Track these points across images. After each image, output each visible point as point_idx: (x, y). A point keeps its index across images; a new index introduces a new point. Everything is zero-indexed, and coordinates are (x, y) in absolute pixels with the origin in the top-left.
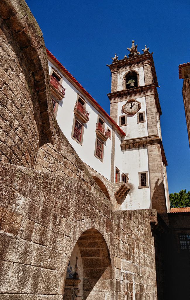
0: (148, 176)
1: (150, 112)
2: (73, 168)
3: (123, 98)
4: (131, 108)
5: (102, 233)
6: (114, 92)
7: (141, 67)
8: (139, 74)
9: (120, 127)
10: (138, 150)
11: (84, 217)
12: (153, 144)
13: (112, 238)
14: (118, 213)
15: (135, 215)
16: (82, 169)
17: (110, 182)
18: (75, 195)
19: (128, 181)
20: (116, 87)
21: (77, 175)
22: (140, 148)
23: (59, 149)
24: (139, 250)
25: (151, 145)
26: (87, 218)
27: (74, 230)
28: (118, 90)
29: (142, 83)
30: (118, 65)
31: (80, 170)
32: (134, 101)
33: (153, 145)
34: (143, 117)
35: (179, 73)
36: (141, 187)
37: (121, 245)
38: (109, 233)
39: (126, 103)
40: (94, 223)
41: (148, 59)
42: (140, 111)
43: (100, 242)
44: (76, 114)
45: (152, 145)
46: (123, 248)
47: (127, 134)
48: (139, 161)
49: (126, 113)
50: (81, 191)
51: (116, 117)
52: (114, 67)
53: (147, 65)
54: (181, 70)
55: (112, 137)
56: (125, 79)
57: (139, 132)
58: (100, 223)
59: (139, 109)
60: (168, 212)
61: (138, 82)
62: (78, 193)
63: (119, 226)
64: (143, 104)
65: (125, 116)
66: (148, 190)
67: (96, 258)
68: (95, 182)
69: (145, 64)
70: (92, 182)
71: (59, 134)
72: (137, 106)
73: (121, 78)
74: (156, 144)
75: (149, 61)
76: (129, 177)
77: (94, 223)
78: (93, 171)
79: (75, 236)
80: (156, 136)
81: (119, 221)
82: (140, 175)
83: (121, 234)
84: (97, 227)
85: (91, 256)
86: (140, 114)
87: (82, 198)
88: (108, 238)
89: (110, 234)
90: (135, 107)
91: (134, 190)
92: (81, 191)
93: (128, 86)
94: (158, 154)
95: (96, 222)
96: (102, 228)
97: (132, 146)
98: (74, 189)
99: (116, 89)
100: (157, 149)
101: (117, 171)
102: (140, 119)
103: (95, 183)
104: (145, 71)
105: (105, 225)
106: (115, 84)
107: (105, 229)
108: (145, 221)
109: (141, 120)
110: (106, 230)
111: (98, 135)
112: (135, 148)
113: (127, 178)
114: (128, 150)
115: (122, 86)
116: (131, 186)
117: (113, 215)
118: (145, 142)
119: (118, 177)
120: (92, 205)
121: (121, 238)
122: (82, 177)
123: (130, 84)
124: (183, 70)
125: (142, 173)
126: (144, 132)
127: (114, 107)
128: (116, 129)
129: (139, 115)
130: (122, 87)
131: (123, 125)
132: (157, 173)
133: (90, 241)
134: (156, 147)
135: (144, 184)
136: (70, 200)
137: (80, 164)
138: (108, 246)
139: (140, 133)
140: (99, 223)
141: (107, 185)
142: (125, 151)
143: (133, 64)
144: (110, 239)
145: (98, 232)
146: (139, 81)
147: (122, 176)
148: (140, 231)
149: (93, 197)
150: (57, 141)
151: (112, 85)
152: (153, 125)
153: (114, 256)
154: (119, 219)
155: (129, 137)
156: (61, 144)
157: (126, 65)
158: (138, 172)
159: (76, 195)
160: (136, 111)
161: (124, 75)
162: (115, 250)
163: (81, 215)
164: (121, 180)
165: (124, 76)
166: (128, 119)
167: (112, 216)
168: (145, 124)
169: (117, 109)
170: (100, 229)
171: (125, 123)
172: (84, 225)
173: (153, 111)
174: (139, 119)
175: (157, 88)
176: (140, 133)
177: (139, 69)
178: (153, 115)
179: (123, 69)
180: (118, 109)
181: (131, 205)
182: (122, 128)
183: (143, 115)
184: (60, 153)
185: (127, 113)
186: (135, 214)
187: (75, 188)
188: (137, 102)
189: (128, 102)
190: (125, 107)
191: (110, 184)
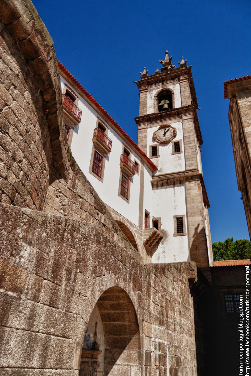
1: (188, 140)
2: (92, 211)
3: (154, 123)
4: (165, 135)
5: (127, 291)
6: (143, 115)
7: (177, 84)
8: (174, 93)
9: (150, 159)
10: (173, 188)
11: (106, 272)
13: (140, 299)
14: (148, 267)
15: (170, 270)
16: (103, 211)
17: (138, 228)
18: (94, 245)
19: (160, 228)
20: (145, 109)
21: (97, 220)
22: (176, 185)
23: (73, 187)
24: (174, 314)
25: (189, 182)
26: (109, 274)
27: (93, 288)
28: (148, 113)
29: (177, 104)
30: (148, 82)
31: (100, 213)
32: (168, 126)
33: (192, 182)
34: (179, 147)
35: (225, 91)
36: (176, 234)
37: (151, 308)
38: (137, 292)
40: (118, 280)
41: (186, 74)
42: (176, 139)
43: (126, 304)
44: (95, 143)
45: (190, 181)
46: (154, 310)
47: (159, 169)
48: (175, 201)
49: (158, 142)
50: (102, 239)
51: (146, 146)
52: (142, 83)
53: (184, 81)
54: (227, 87)
55: (141, 171)
56: (157, 99)
57: (175, 165)
58: (125, 280)
59: (175, 136)
60: (211, 265)
61: (173, 103)
62: (98, 242)
63: (149, 284)
64: (180, 131)
65: (156, 146)
66: (185, 238)
67: (120, 323)
68: (119, 228)
70: (115, 228)
71: (75, 168)
72: (171, 133)
73: (151, 97)
74: (195, 181)
75: (187, 76)
76: (162, 221)
77: (117, 279)
78: (116, 214)
79: (94, 296)
80: (196, 170)
81: (149, 278)
82: (176, 220)
83: (152, 294)
84: (122, 284)
85: (114, 321)
86: (176, 142)
87: (102, 248)
88: (135, 298)
89: (138, 293)
90: (169, 134)
91: (168, 239)
92: (102, 239)
93: (161, 108)
94: (198, 193)
95: (120, 279)
96: (128, 286)
97: (166, 183)
98: (93, 237)
99: (145, 111)
100: (197, 187)
101: (147, 215)
102: (175, 149)
103: (119, 230)
104: (182, 88)
105: (132, 282)
106: (144, 106)
107: (131, 287)
108: (181, 277)
109: (177, 150)
110: (133, 288)
111: (122, 169)
112: (169, 186)
113: (159, 223)
114: (160, 188)
116: (164, 233)
117: (142, 269)
118: (182, 178)
119: (148, 222)
120: (115, 257)
121: (152, 299)
122: (102, 221)
123: (162, 106)
124: (229, 87)
125: (178, 217)
127: (143, 135)
128: (146, 161)
129: (174, 144)
130: (153, 109)
131: (154, 157)
132: (197, 217)
133: (112, 302)
134: (195, 184)
135: (180, 230)
136: (88, 251)
137: (101, 205)
138: (136, 308)
139: (175, 166)
140: (125, 279)
141: (134, 232)
142: (157, 189)
143: (167, 80)
144: (138, 299)
145: (123, 291)
146: (174, 102)
147: (153, 221)
148: (176, 290)
149: (117, 247)
150: (71, 176)
151: (140, 107)
152: (191, 156)
153: (143, 321)
154: (149, 274)
155: (162, 172)
156: (77, 181)
157: (158, 82)
158: (174, 216)
159: (95, 245)
160: (171, 139)
161: (155, 94)
162: (144, 313)
163: (102, 270)
164: (151, 226)
165: (156, 96)
166: (161, 150)
167: (140, 270)
168: (182, 155)
169: (147, 137)
170: (125, 286)
171: (157, 155)
172: (105, 283)
173: (192, 139)
174: (174, 150)
175: (197, 110)
176: (175, 166)
177: (174, 87)
178: (192, 145)
179: (154, 87)
181: (165, 257)
182: (153, 160)
183: (179, 144)
184: (75, 191)
185: (159, 142)
186: (170, 268)
187: (94, 235)
188: (172, 127)
189: (161, 128)
190: (157, 134)
191: (138, 230)
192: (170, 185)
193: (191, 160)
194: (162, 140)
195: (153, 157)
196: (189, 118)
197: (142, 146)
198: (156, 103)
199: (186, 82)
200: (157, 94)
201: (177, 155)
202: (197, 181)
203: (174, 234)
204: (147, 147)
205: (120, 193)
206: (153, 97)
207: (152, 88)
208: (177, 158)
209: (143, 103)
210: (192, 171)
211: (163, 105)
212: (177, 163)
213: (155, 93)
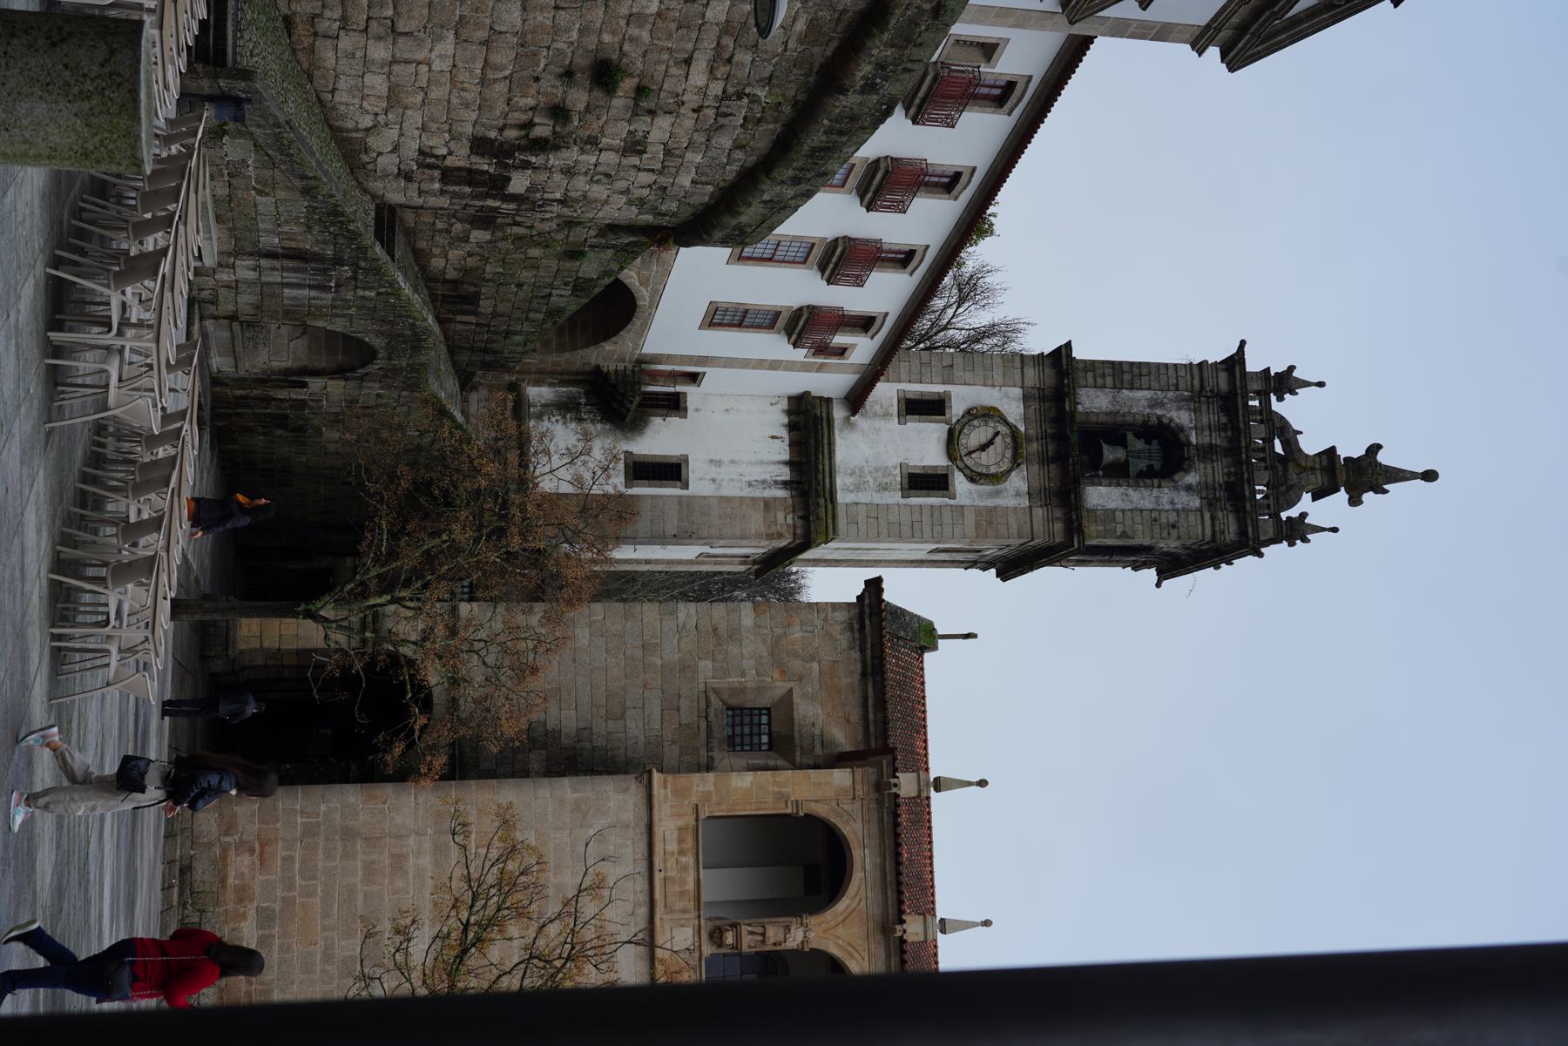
0: (670, 491)
7: (1201, 498)
12: (793, 518)
17: (638, 352)
30: (1236, 395)
39: (1011, 420)
48: (733, 462)
55: (822, 364)
57: (861, 470)
59: (972, 480)
69: (1213, 519)
76: (674, 420)
78: (652, 297)
82: (675, 461)
99: (1100, 381)
101: (694, 378)
115: (1111, 408)
125: (683, 468)
126: (858, 488)
146: (1119, 485)
152: (883, 523)
155: (841, 430)
156: (611, 250)
157: (1229, 433)
161: (1171, 420)
165: (1165, 421)
168: (894, 497)
171: (908, 417)
177: (1189, 488)
180: (989, 388)
188: (1009, 471)
189: (1014, 432)
192: (791, 452)
193: (872, 520)
194: (962, 436)
195: (903, 402)
196: (1035, 530)
197: (952, 366)
198: (1129, 419)
199: (1200, 532)
200: (1172, 425)
201: (899, 479)
202: (792, 531)
203: (631, 453)
204: (943, 383)
205: (719, 305)
206: (1159, 412)
207: (1204, 408)
208: (885, 480)
209: (1141, 375)
210: (830, 521)
211: (1126, 447)
212: (869, 478)
213: (1177, 420)
